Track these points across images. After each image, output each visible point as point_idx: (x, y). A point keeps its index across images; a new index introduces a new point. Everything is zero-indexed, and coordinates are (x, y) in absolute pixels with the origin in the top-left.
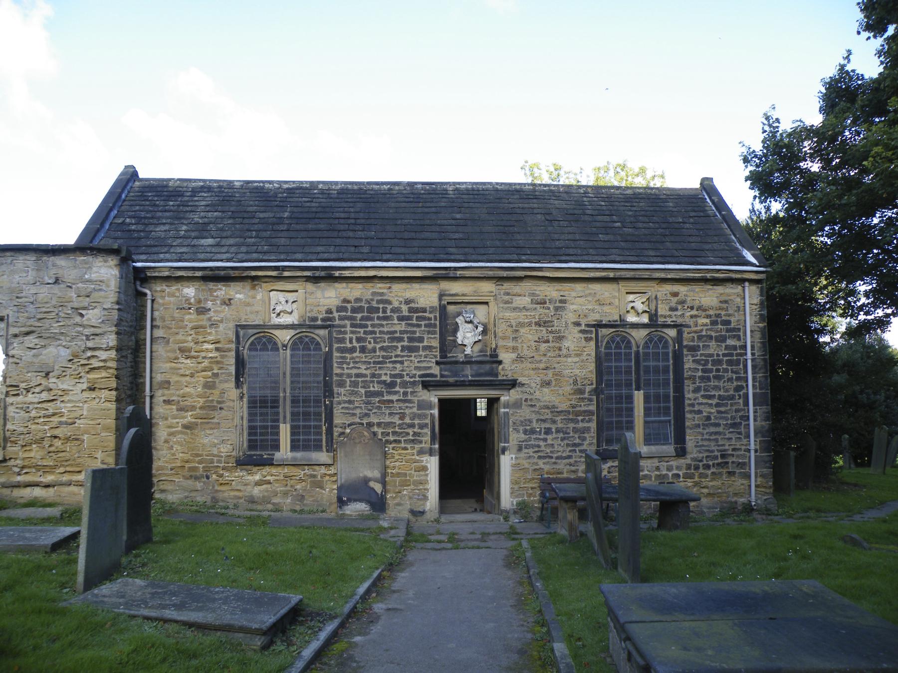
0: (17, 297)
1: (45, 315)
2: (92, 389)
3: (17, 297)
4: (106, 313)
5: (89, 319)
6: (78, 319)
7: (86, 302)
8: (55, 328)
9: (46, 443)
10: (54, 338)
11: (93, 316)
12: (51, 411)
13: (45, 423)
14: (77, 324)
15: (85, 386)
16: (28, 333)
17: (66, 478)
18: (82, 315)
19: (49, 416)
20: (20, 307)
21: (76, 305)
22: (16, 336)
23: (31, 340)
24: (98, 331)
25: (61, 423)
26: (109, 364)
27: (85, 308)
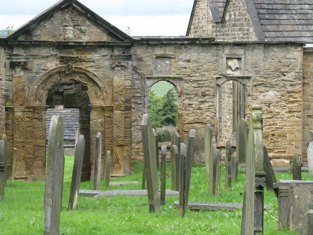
0: (256, 67)
1: (268, 76)
2: (290, 112)
3: (256, 67)
4: (296, 74)
5: (288, 77)
6: (283, 78)
7: (287, 69)
8: (273, 82)
9: (270, 138)
10: (272, 86)
11: (290, 76)
12: (272, 123)
13: (269, 129)
14: (283, 80)
15: (287, 110)
16: (260, 85)
17: (277, 155)
18: (284, 75)
19: (271, 125)
20: (257, 72)
21: (283, 70)
22: (255, 86)
23: (262, 89)
24: (292, 83)
25: (276, 128)
26: (298, 99)
27: (287, 72)
